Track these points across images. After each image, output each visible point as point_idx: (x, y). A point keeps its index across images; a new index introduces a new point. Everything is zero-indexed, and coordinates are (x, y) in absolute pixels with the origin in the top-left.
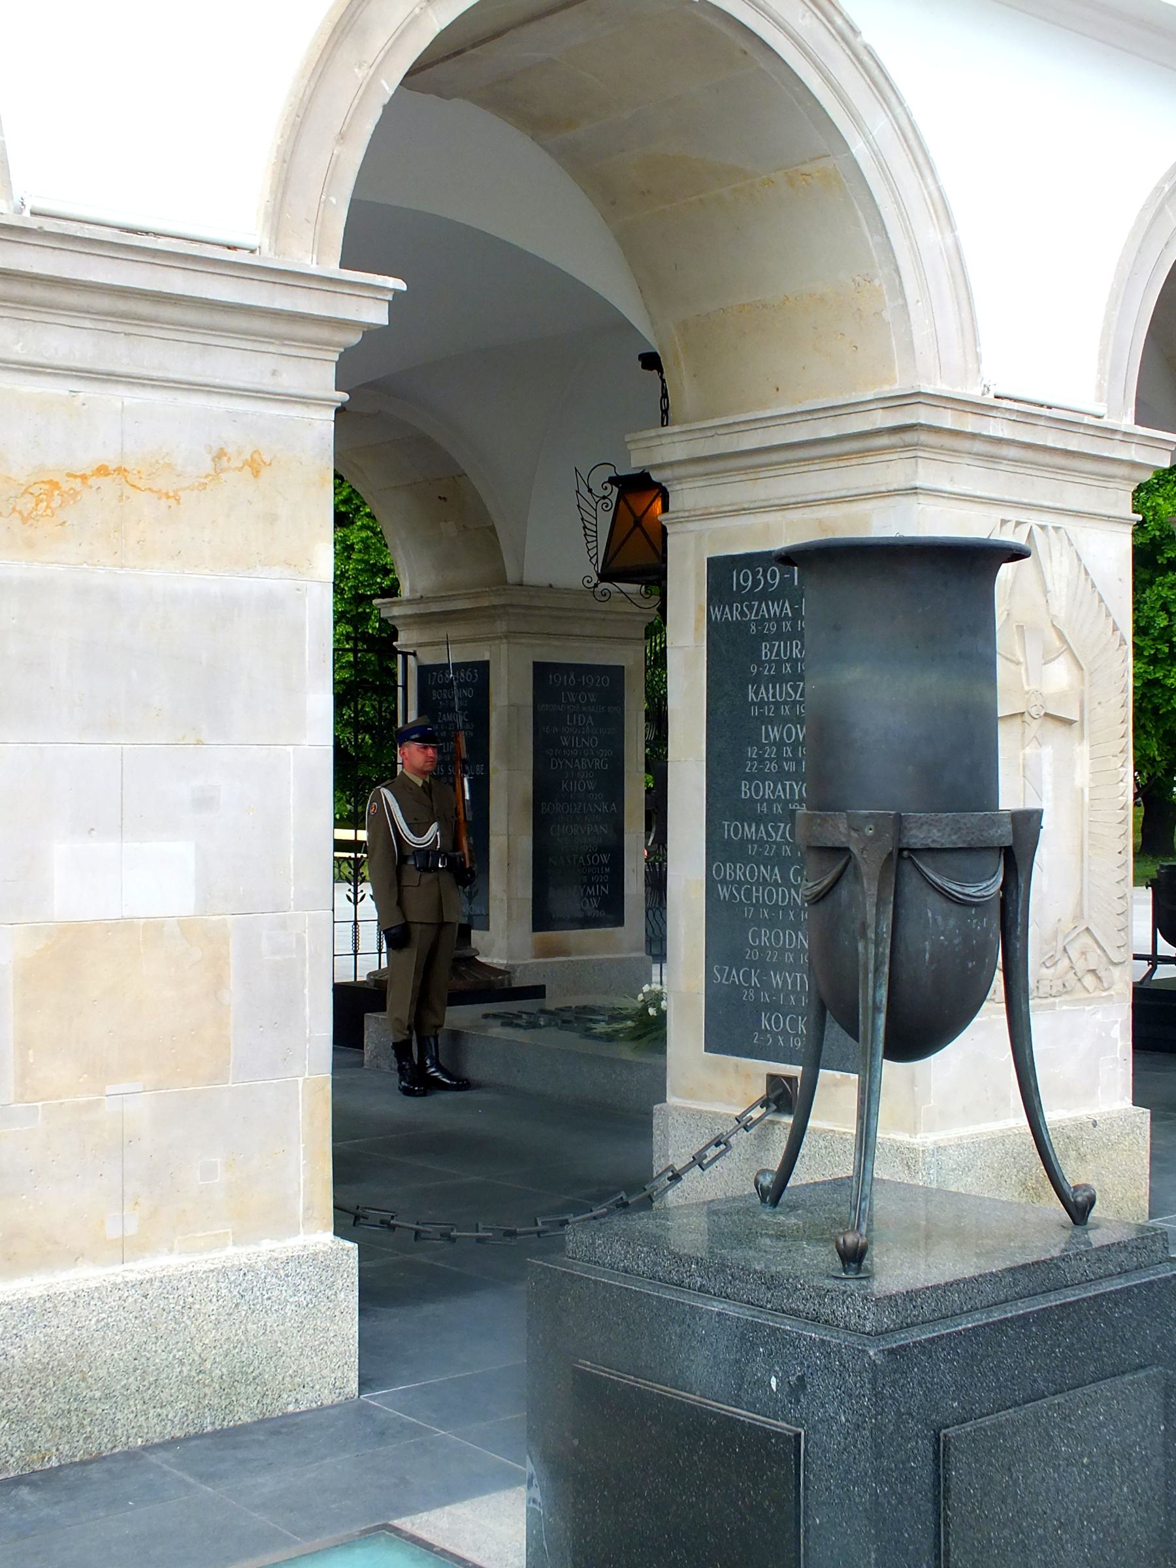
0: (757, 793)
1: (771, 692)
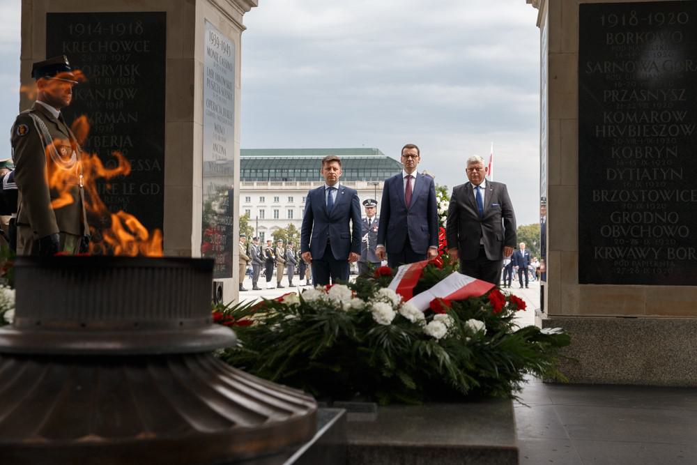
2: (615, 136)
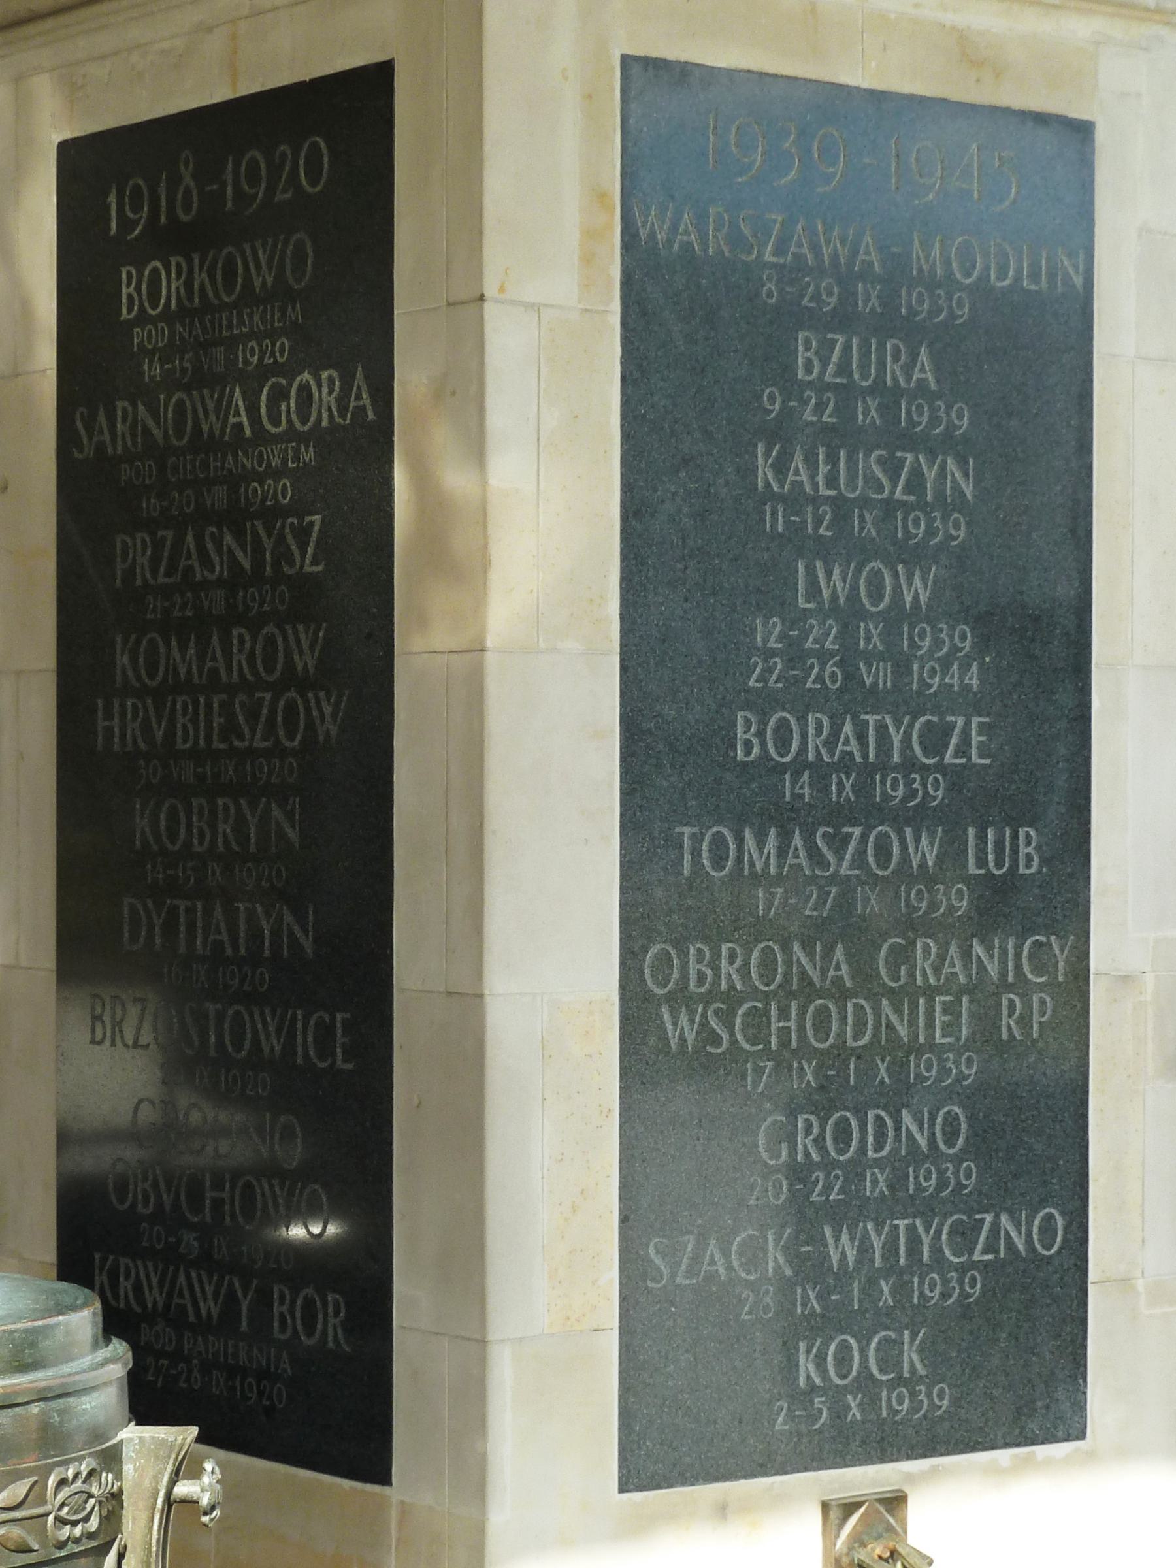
0: (783, 745)
1: (823, 469)
2: (142, 745)
